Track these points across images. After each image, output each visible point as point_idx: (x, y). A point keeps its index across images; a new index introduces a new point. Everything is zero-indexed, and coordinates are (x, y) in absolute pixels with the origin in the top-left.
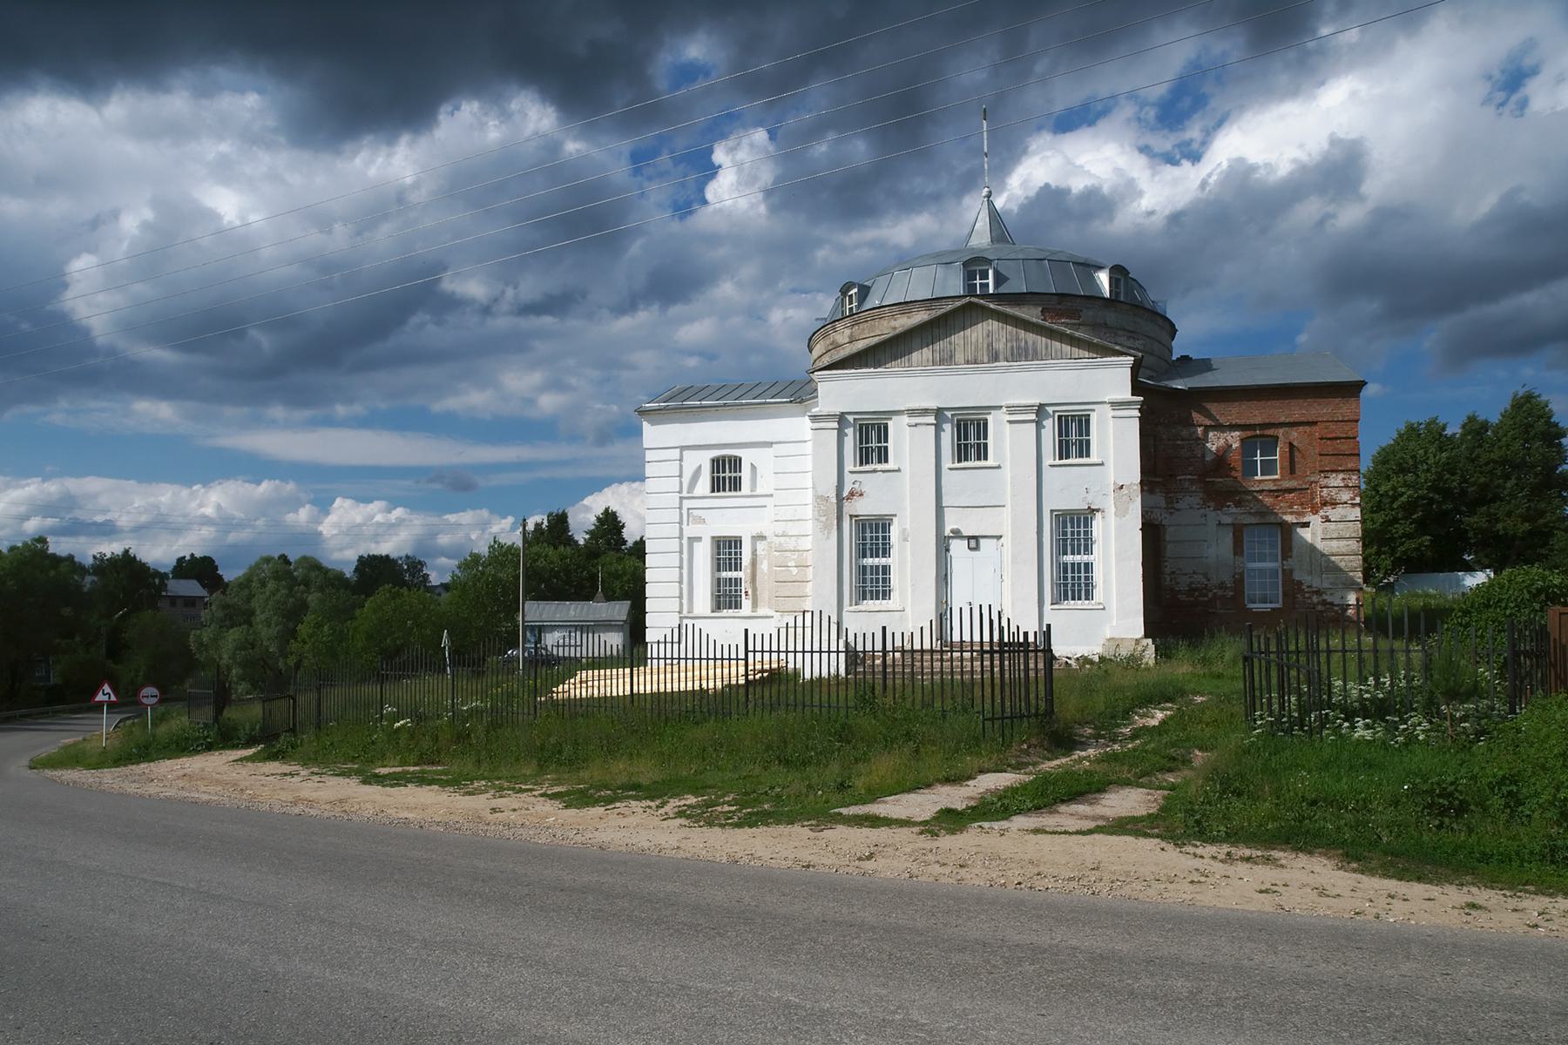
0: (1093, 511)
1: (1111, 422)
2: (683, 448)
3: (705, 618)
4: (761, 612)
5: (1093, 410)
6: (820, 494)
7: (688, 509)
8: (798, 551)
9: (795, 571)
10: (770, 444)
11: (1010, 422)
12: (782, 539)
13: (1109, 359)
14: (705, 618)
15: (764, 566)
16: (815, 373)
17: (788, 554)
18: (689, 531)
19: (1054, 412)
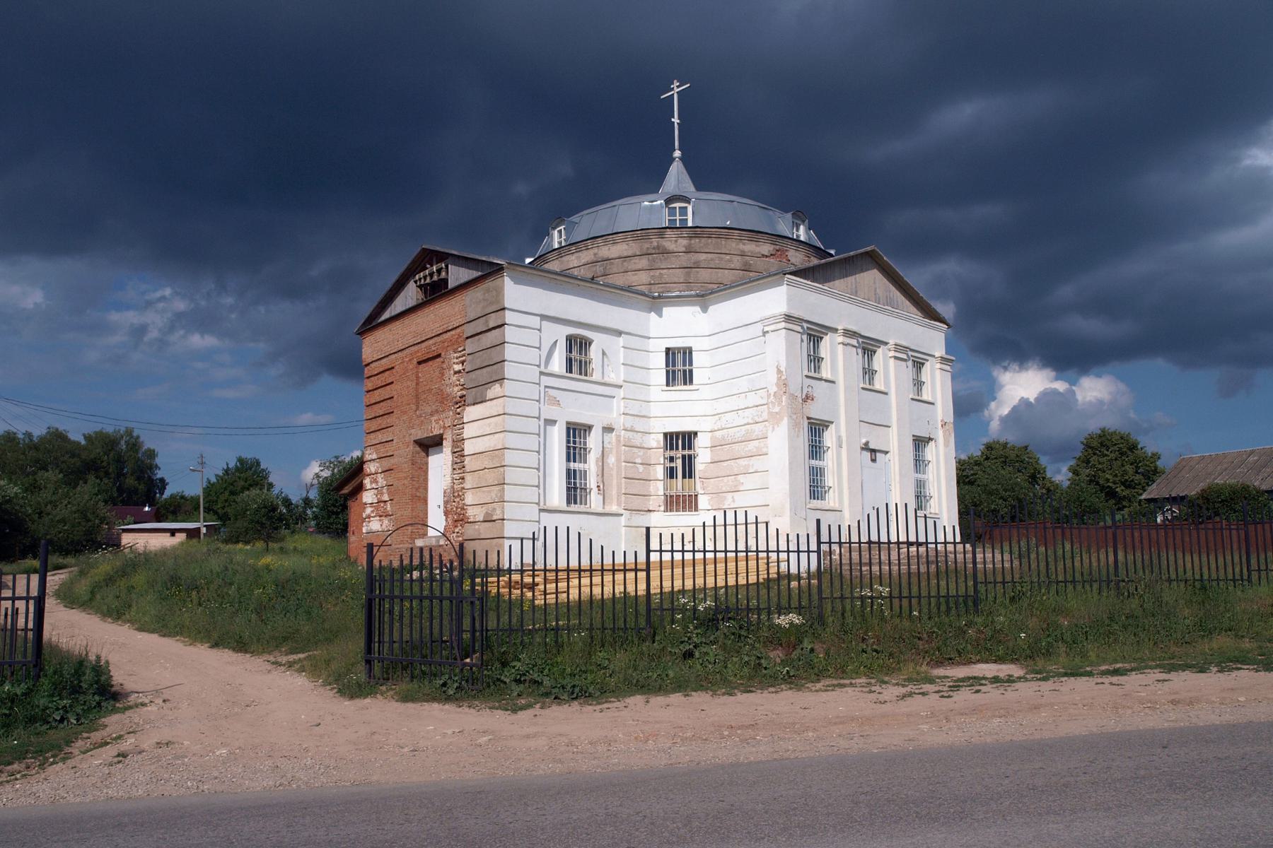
0: (930, 439)
1: (938, 372)
2: (544, 317)
3: (561, 512)
4: (614, 508)
5: (927, 360)
6: (792, 392)
7: (546, 387)
8: (643, 448)
9: (641, 468)
10: (619, 333)
11: (896, 358)
12: (630, 434)
13: (932, 322)
14: (561, 512)
15: (611, 460)
16: (787, 276)
17: (635, 450)
18: (548, 412)
19: (912, 356)
